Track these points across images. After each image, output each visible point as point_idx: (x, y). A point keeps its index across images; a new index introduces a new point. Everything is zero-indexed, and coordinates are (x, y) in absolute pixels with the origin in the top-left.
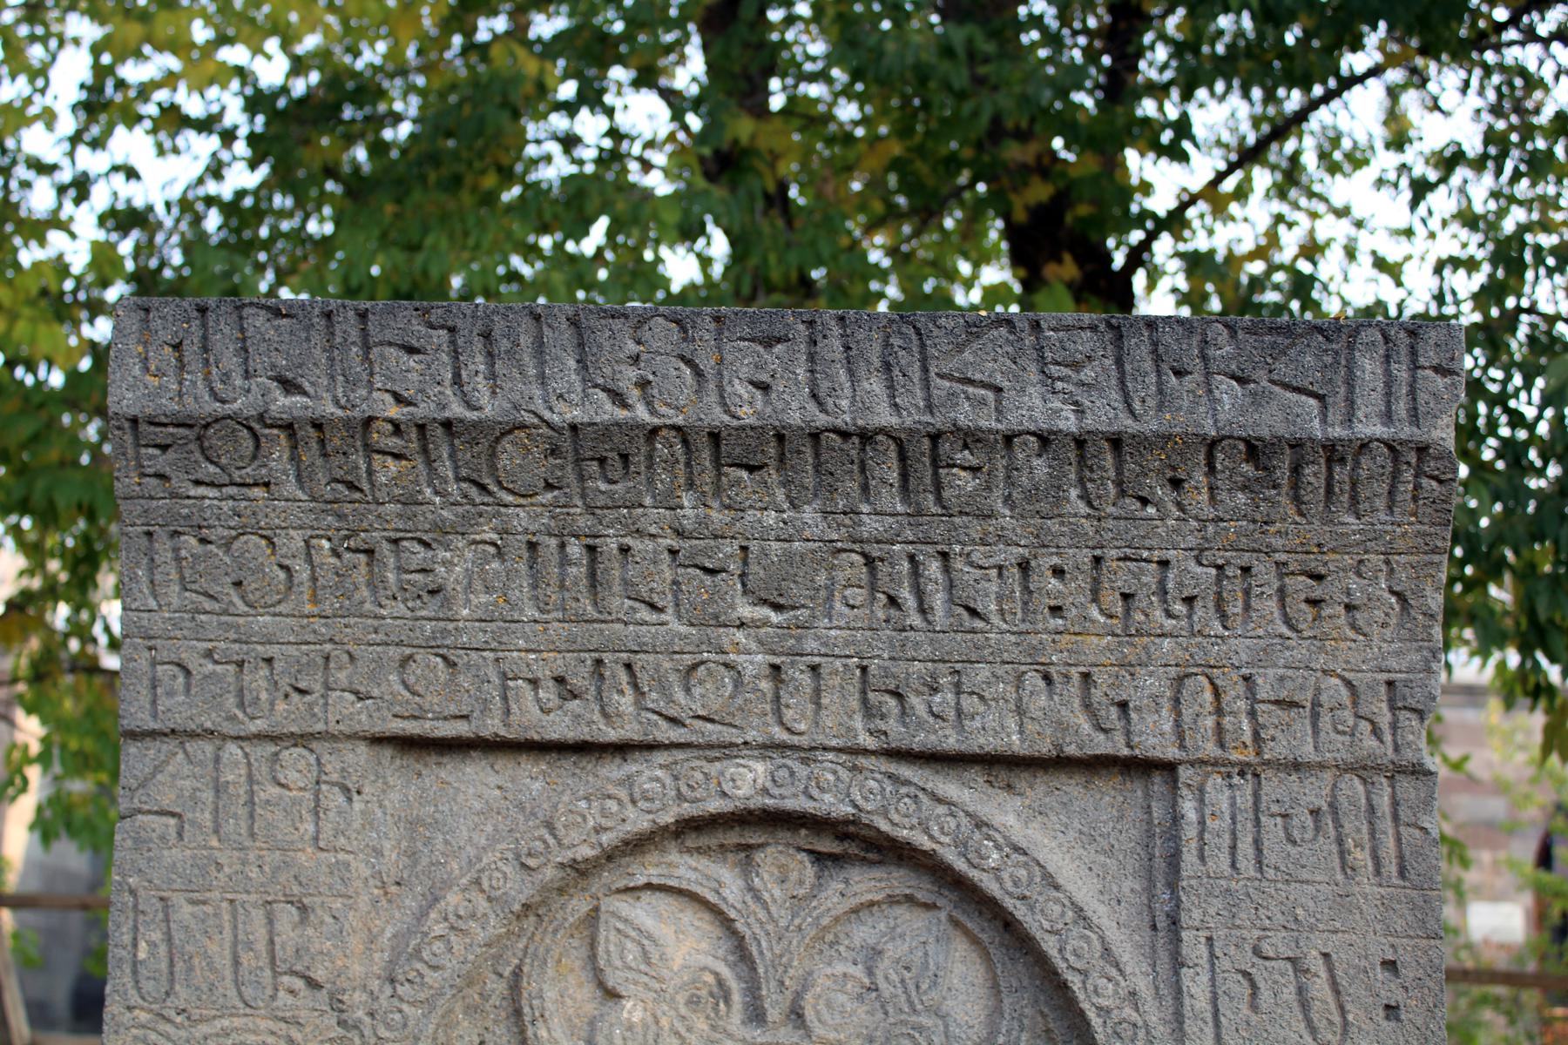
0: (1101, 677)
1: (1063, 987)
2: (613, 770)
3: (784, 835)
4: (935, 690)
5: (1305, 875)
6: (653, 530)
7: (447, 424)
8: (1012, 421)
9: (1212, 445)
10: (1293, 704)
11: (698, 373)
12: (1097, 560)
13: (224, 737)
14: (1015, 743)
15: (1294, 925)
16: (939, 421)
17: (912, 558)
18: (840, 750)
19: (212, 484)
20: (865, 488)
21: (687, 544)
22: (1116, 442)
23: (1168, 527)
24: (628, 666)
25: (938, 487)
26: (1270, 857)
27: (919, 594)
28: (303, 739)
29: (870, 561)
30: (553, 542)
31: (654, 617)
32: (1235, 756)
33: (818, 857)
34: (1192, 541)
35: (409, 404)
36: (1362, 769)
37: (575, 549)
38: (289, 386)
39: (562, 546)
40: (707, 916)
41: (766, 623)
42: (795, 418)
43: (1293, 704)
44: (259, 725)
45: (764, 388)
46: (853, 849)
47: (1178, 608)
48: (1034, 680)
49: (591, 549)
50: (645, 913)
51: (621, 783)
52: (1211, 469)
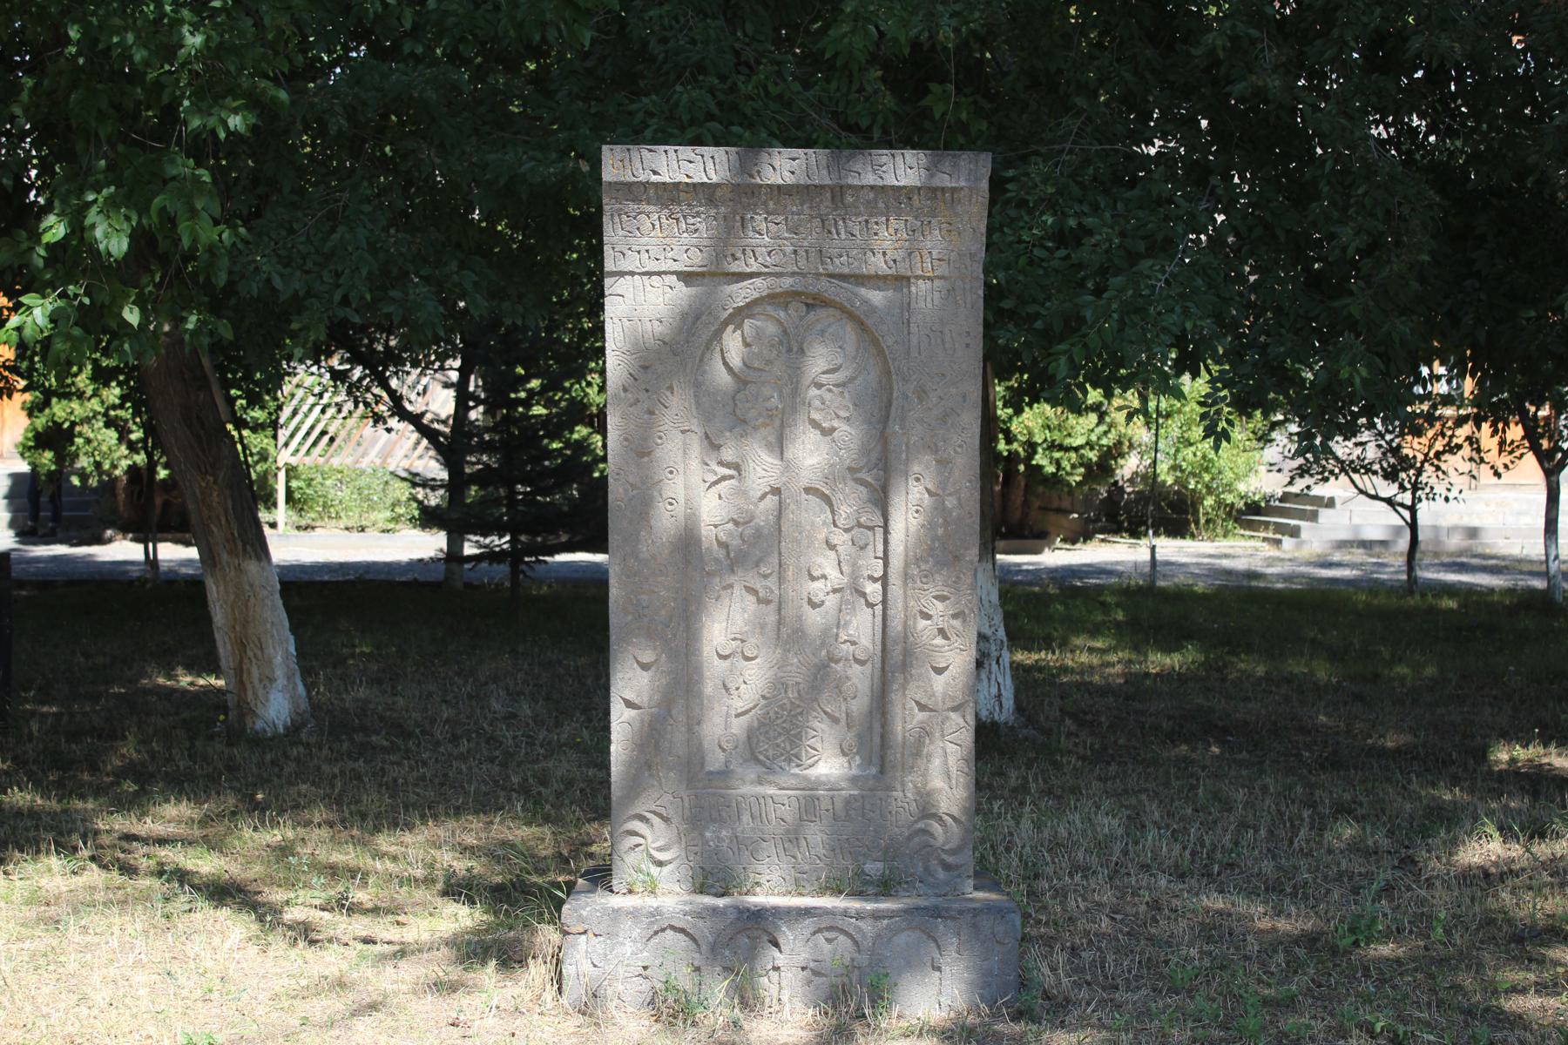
8: (865, 182)
28: (659, 274)
38: (655, 173)
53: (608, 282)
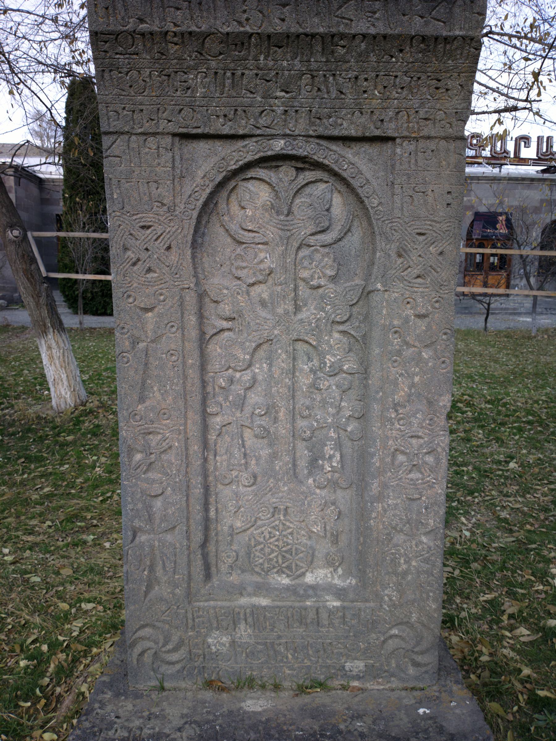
0: (377, 112)
1: (362, 202)
2: (240, 144)
3: (288, 163)
4: (331, 117)
5: (429, 169)
6: (251, 68)
7: (190, 33)
9: (412, 38)
10: (430, 119)
11: (264, 16)
12: (377, 76)
13: (131, 134)
14: (353, 133)
15: (425, 183)
16: (334, 30)
17: (325, 76)
18: (304, 136)
19: (121, 54)
20: (312, 53)
21: (260, 72)
22: (385, 37)
23: (398, 63)
24: (245, 111)
25: (333, 52)
26: (420, 164)
27: (327, 87)
28: (154, 134)
29: (313, 77)
30: (223, 72)
31: (252, 96)
32: (413, 135)
33: (297, 169)
34: (405, 69)
35: (179, 26)
36: (446, 138)
37: (229, 74)
39: (225, 73)
40: (267, 186)
41: (283, 97)
42: (293, 30)
43: (430, 119)
44: (140, 131)
45: (283, 20)
46: (307, 166)
47: (399, 90)
48: (357, 113)
49: (233, 74)
50: (251, 186)
51: (243, 147)
52: (411, 45)
53: (106, 141)
